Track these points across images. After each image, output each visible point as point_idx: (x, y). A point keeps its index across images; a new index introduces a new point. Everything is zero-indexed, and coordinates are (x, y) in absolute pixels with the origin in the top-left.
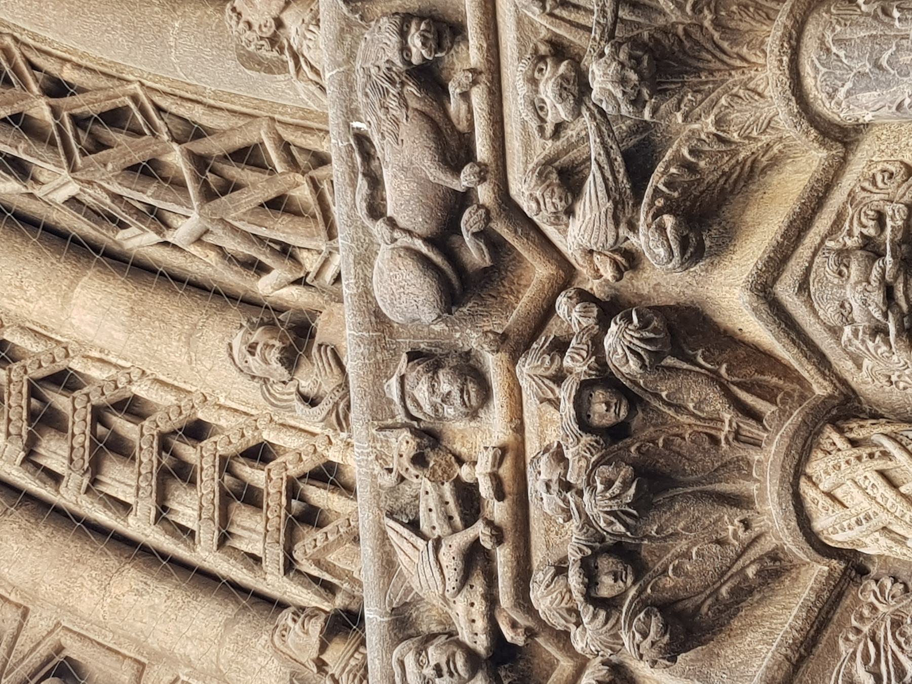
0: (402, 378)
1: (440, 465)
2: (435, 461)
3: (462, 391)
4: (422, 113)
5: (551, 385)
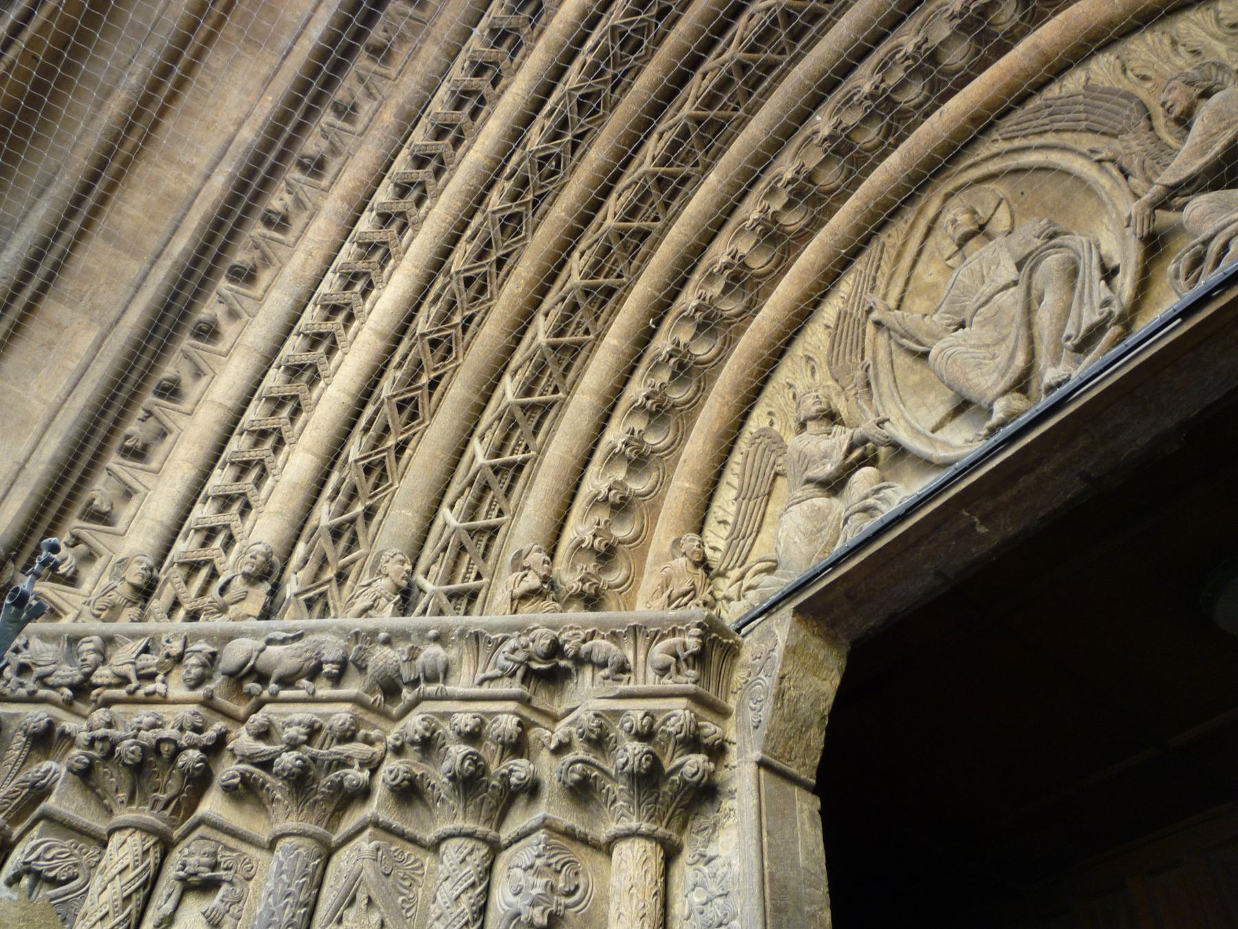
0: (200, 651)
4: (301, 669)
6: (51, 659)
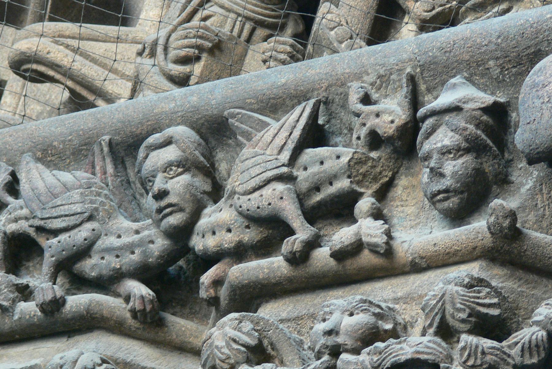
0: (455, 109)
1: (373, 167)
2: (380, 158)
3: (446, 191)
5: (435, 324)
6: (77, 208)
